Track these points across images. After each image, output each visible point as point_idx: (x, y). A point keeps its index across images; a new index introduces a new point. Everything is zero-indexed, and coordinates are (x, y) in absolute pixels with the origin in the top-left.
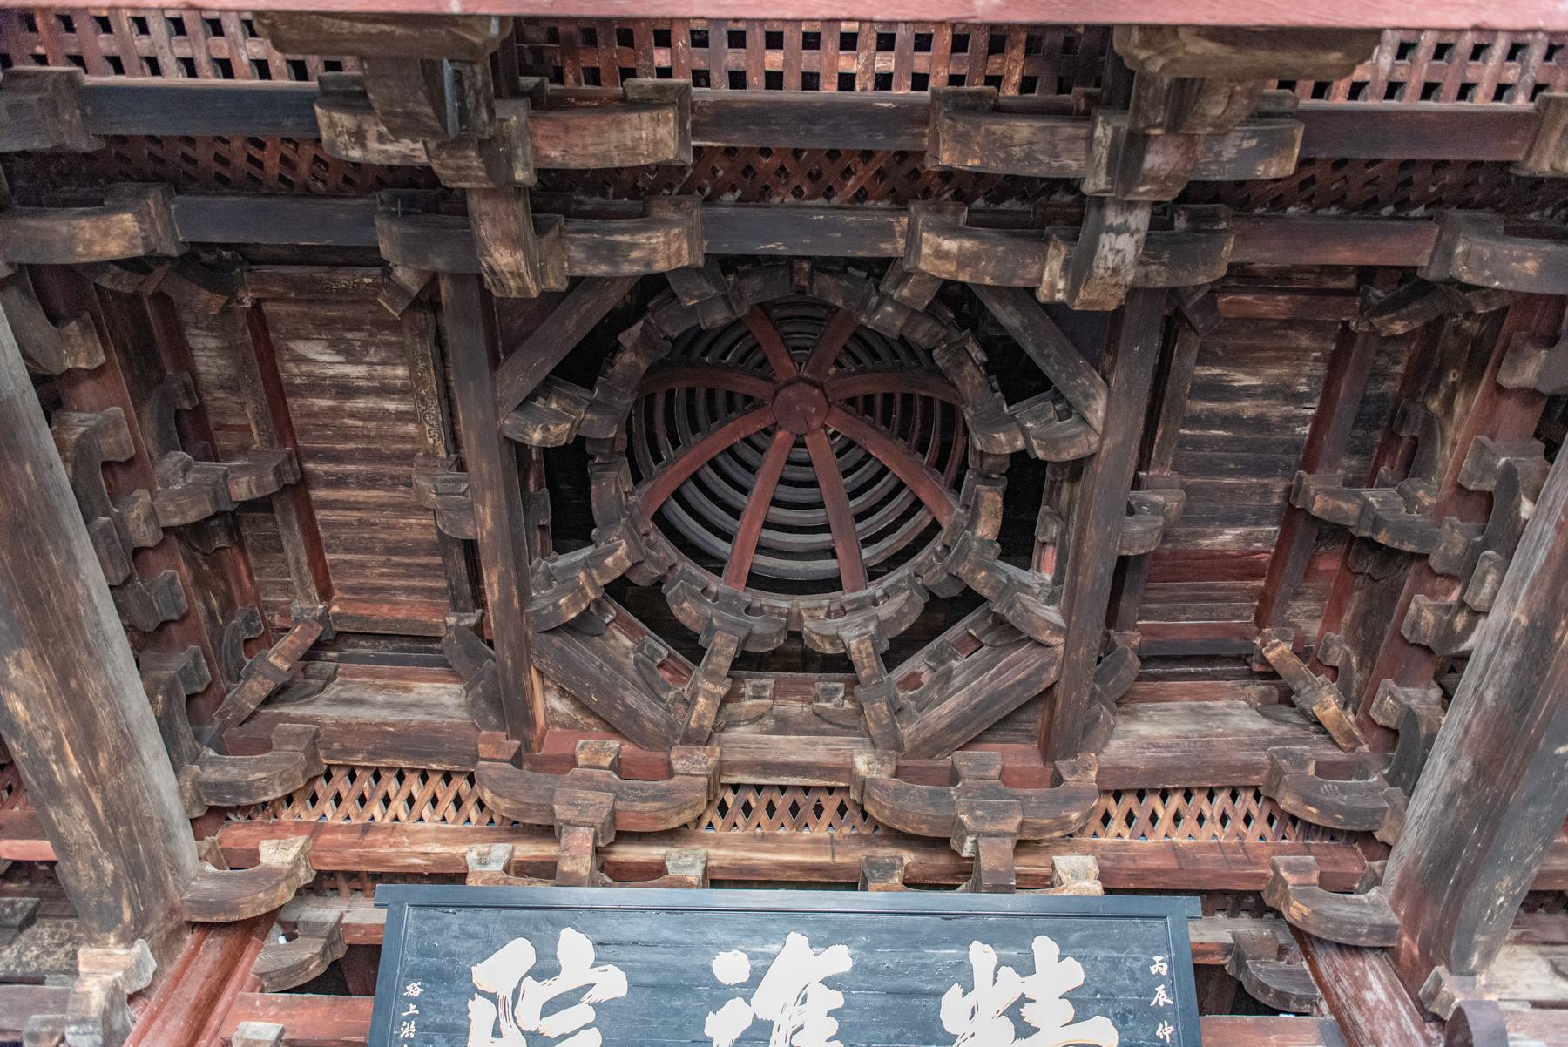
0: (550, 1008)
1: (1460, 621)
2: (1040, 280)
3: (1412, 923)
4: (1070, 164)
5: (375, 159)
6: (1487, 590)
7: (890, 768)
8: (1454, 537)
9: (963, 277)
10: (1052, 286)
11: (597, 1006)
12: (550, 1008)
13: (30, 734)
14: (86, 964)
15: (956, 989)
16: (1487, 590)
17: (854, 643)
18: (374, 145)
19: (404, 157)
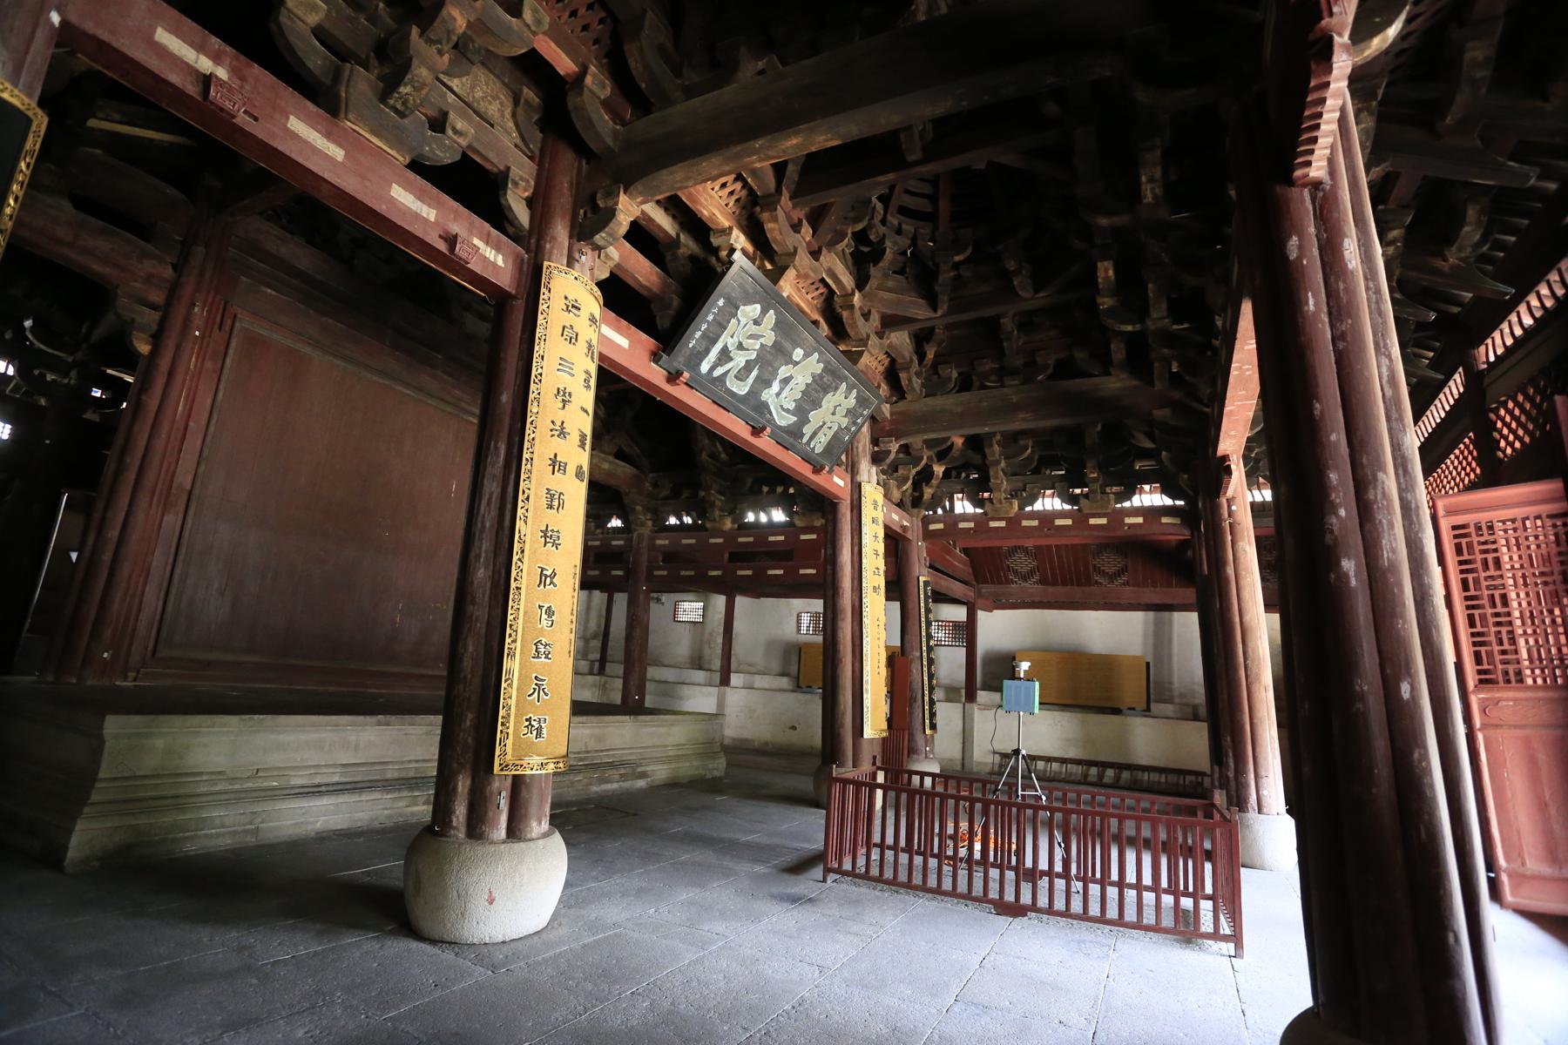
0: (751, 337)
1: (993, 378)
2: (1103, 297)
3: (892, 422)
4: (1155, 315)
5: (1143, 187)
6: (1012, 383)
7: (860, 304)
8: (1019, 362)
9: (1100, 280)
10: (1104, 303)
11: (761, 344)
12: (751, 337)
13: (776, 147)
14: (622, 205)
15: (832, 393)
16: (1012, 383)
17: (888, 250)
18: (1149, 186)
19: (1145, 196)
